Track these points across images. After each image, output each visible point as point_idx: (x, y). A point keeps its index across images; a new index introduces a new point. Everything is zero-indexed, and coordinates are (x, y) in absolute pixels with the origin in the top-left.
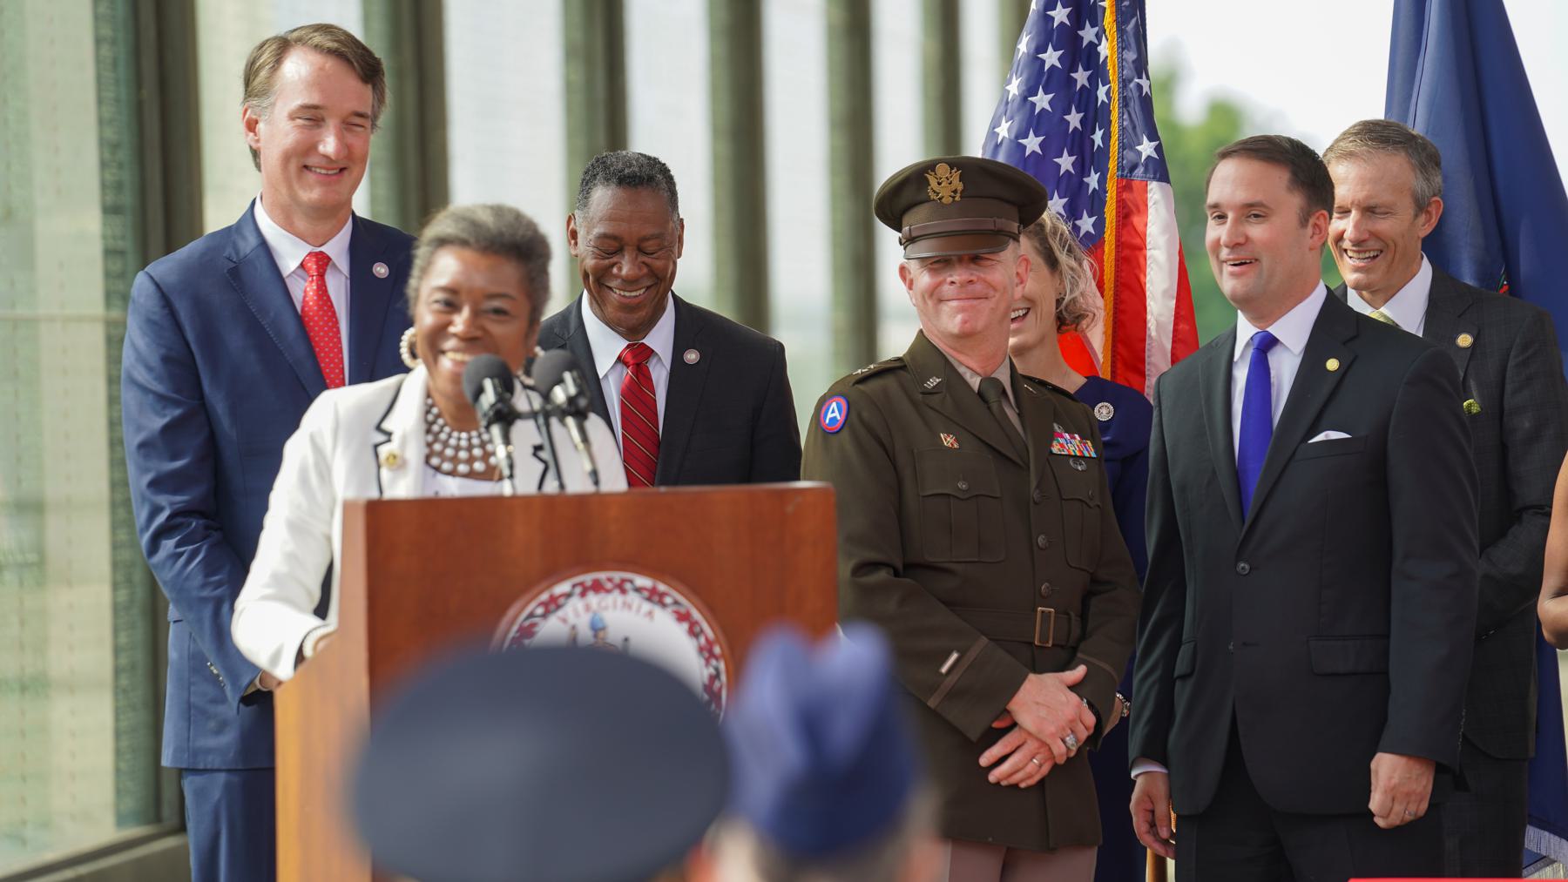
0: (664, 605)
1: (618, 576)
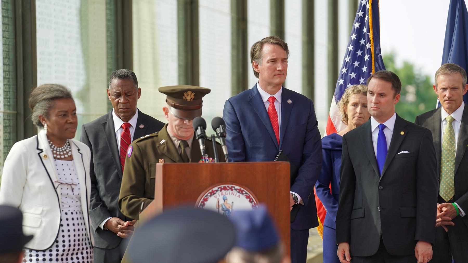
0: (243, 194)
1: (230, 186)
